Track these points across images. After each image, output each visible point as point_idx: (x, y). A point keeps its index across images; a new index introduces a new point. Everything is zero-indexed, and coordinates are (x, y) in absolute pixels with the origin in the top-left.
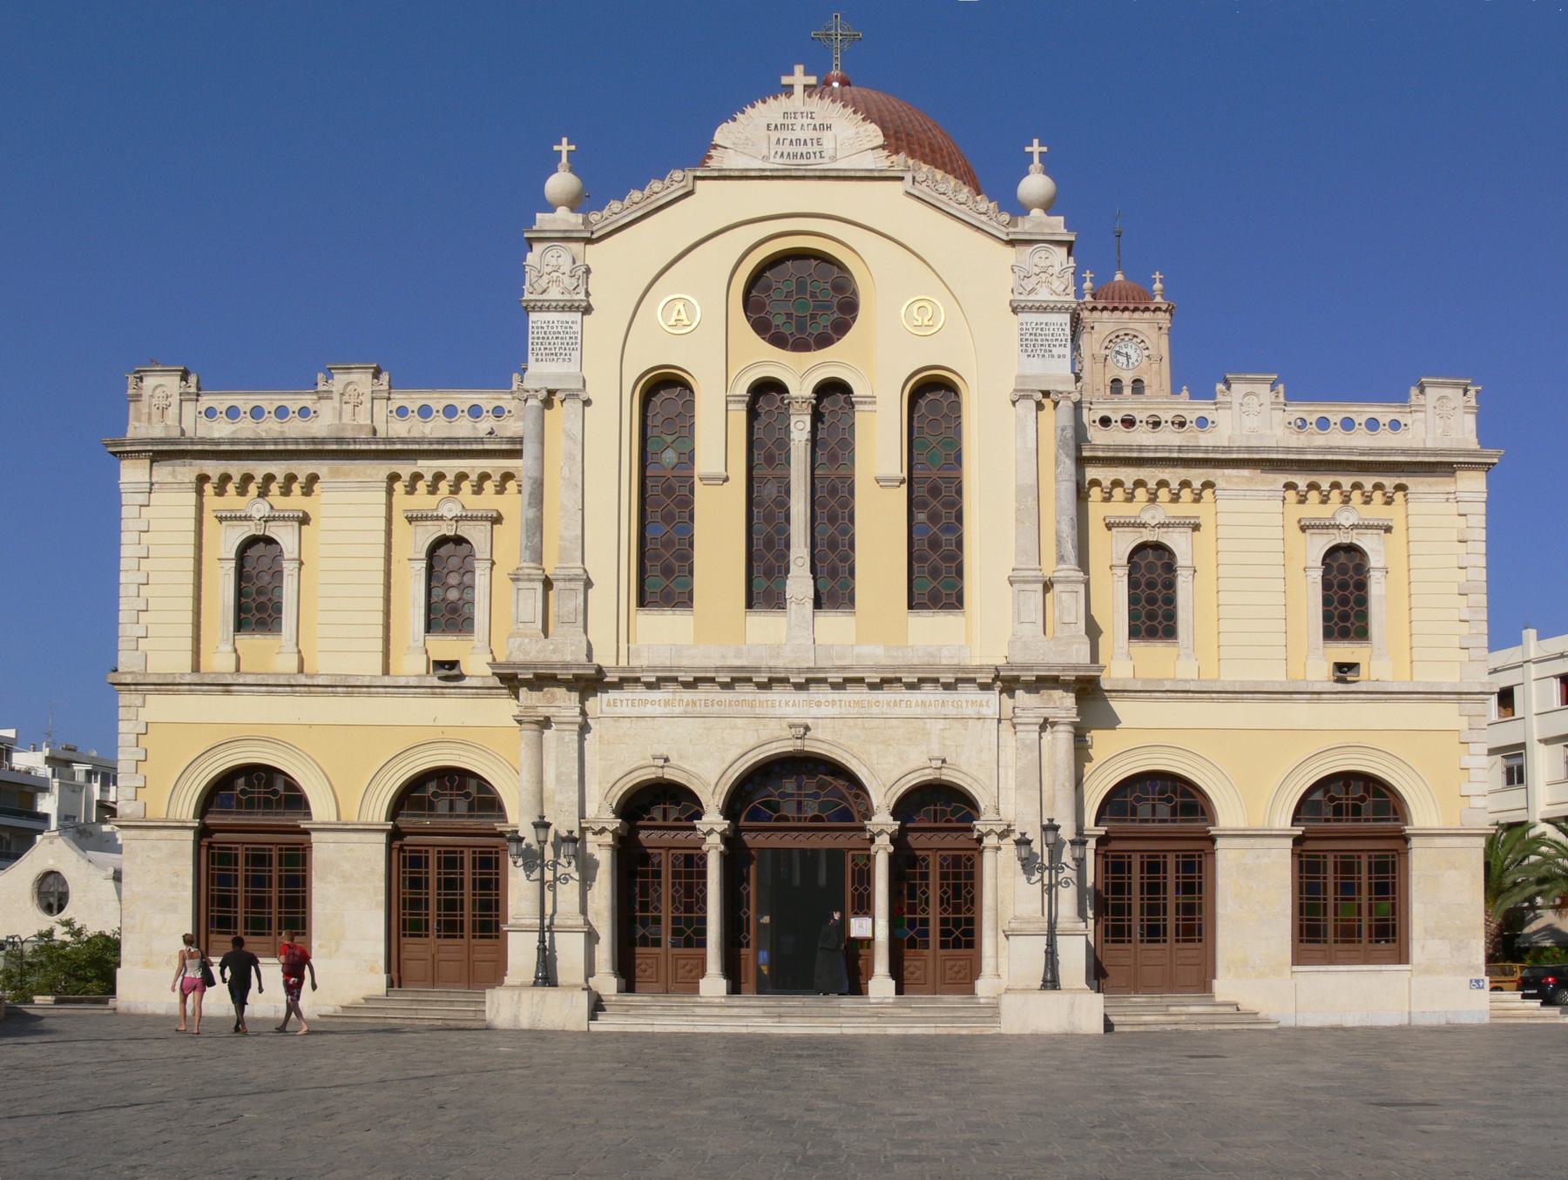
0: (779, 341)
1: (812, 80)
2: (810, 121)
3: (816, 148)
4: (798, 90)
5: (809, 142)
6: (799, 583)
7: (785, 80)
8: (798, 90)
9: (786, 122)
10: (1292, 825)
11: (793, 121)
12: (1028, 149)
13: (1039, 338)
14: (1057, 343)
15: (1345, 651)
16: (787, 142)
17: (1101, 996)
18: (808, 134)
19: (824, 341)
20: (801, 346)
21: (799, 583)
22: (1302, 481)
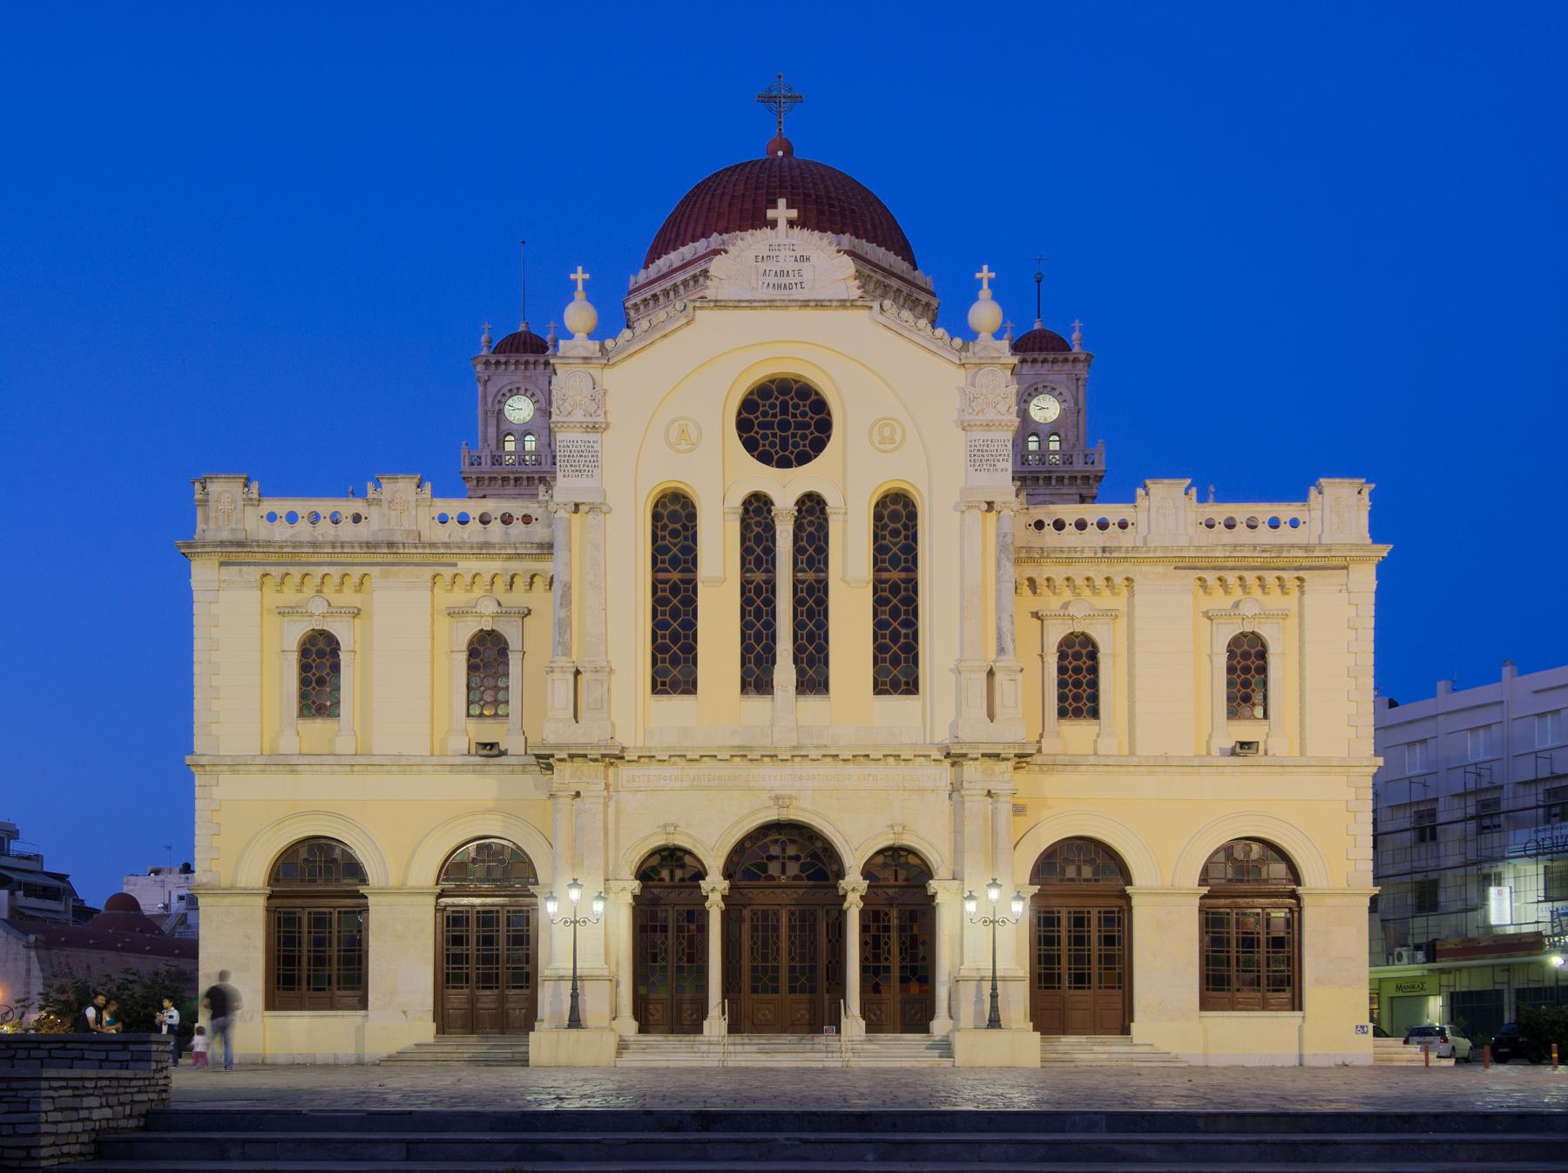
0: (765, 458)
1: (794, 213)
2: (792, 253)
3: (798, 280)
4: (782, 224)
5: (791, 273)
6: (785, 672)
7: (770, 214)
8: (782, 224)
9: (771, 254)
10: (1199, 885)
11: (777, 253)
12: (978, 275)
13: (985, 454)
14: (1001, 458)
15: (1245, 730)
16: (773, 273)
17: (1038, 1034)
18: (791, 265)
19: (803, 459)
20: (784, 463)
21: (785, 672)
22: (1211, 577)
